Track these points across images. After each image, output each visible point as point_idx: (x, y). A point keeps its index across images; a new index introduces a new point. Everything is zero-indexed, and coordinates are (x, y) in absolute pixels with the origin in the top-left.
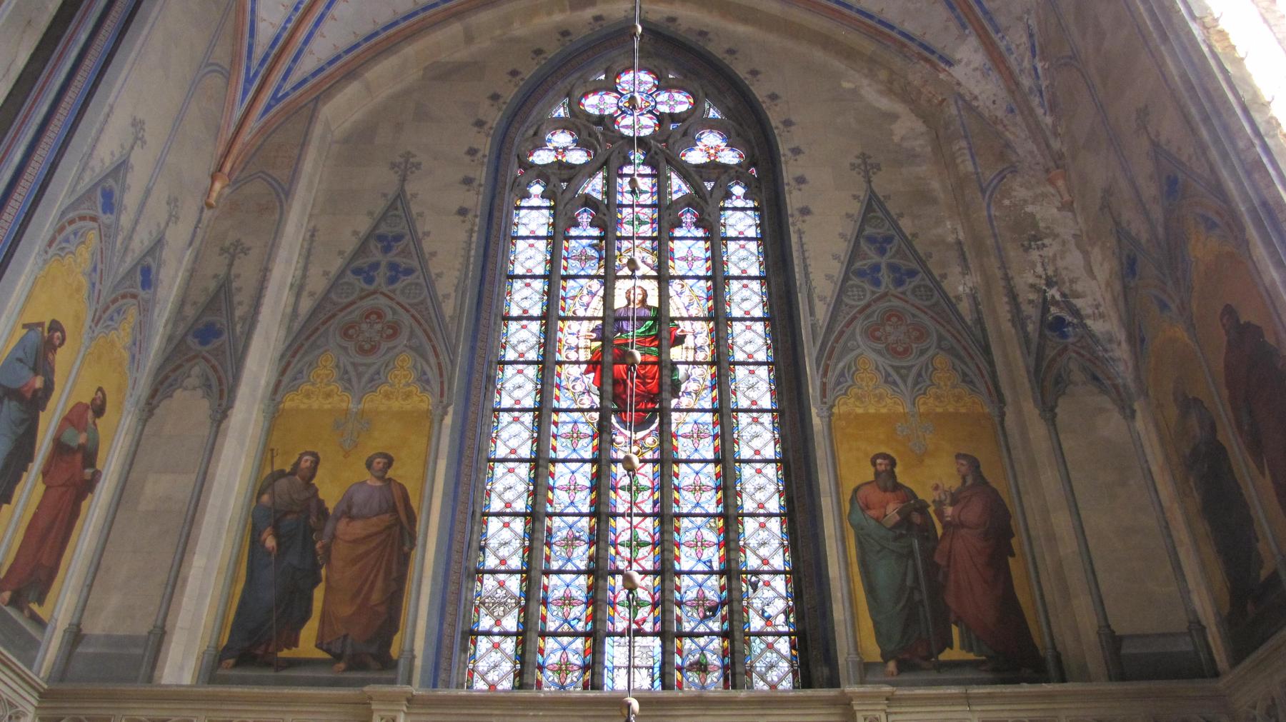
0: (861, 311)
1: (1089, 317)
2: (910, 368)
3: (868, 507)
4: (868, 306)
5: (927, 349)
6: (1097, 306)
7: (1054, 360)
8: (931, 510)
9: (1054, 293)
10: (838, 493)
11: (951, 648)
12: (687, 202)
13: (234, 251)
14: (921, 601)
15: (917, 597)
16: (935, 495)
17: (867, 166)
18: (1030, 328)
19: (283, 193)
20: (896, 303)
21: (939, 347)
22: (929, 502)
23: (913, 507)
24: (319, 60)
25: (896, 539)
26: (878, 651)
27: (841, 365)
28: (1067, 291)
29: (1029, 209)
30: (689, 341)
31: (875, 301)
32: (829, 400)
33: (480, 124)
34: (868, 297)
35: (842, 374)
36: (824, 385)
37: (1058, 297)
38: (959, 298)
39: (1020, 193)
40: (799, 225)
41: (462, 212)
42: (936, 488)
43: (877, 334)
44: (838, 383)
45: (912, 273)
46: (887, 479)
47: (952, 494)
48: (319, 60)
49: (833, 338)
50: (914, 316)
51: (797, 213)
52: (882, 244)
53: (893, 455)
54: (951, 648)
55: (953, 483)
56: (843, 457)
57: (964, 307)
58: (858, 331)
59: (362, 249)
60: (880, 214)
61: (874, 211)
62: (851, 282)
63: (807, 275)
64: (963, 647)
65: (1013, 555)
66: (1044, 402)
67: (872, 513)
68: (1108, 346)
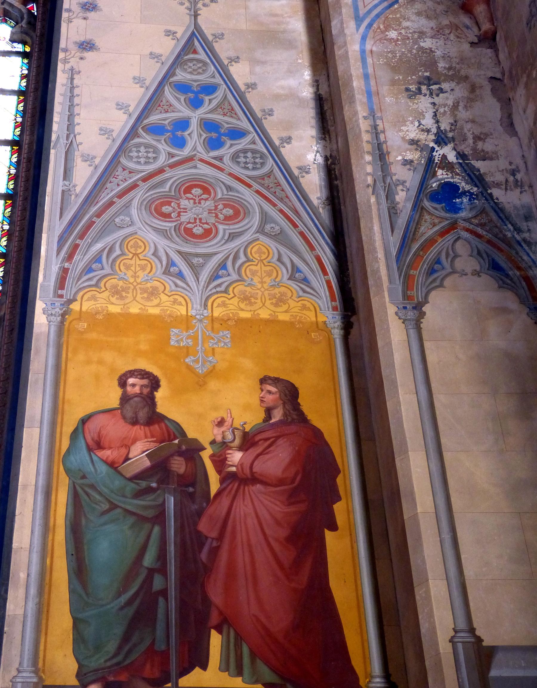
0: (145, 179)
1: (498, 185)
2: (208, 256)
3: (99, 445)
4: (161, 171)
5: (240, 234)
6: (513, 173)
7: (430, 242)
8: (206, 455)
10: (53, 424)
11: (204, 667)
14: (164, 593)
15: (158, 583)
16: (217, 434)
18: (401, 196)
20: (204, 170)
21: (261, 230)
22: (205, 440)
25: (139, 494)
26: (74, 666)
27: (98, 246)
28: (468, 151)
31: (172, 166)
32: (67, 293)
34: (162, 160)
35: (97, 259)
36: (65, 271)
37: (452, 157)
38: (305, 170)
40: (73, 62)
42: (221, 423)
43: (166, 209)
44: (88, 270)
45: (237, 134)
46: (141, 404)
47: (245, 435)
49: (93, 210)
50: (229, 188)
51: (72, 47)
52: (196, 96)
53: (156, 372)
54: (204, 667)
55: (250, 417)
56: (72, 373)
58: (135, 203)
60: (202, 56)
61: (195, 52)
62: (137, 140)
63: (71, 126)
64: (225, 667)
65: (334, 527)
66: (406, 297)
67: (107, 454)
68: (524, 225)
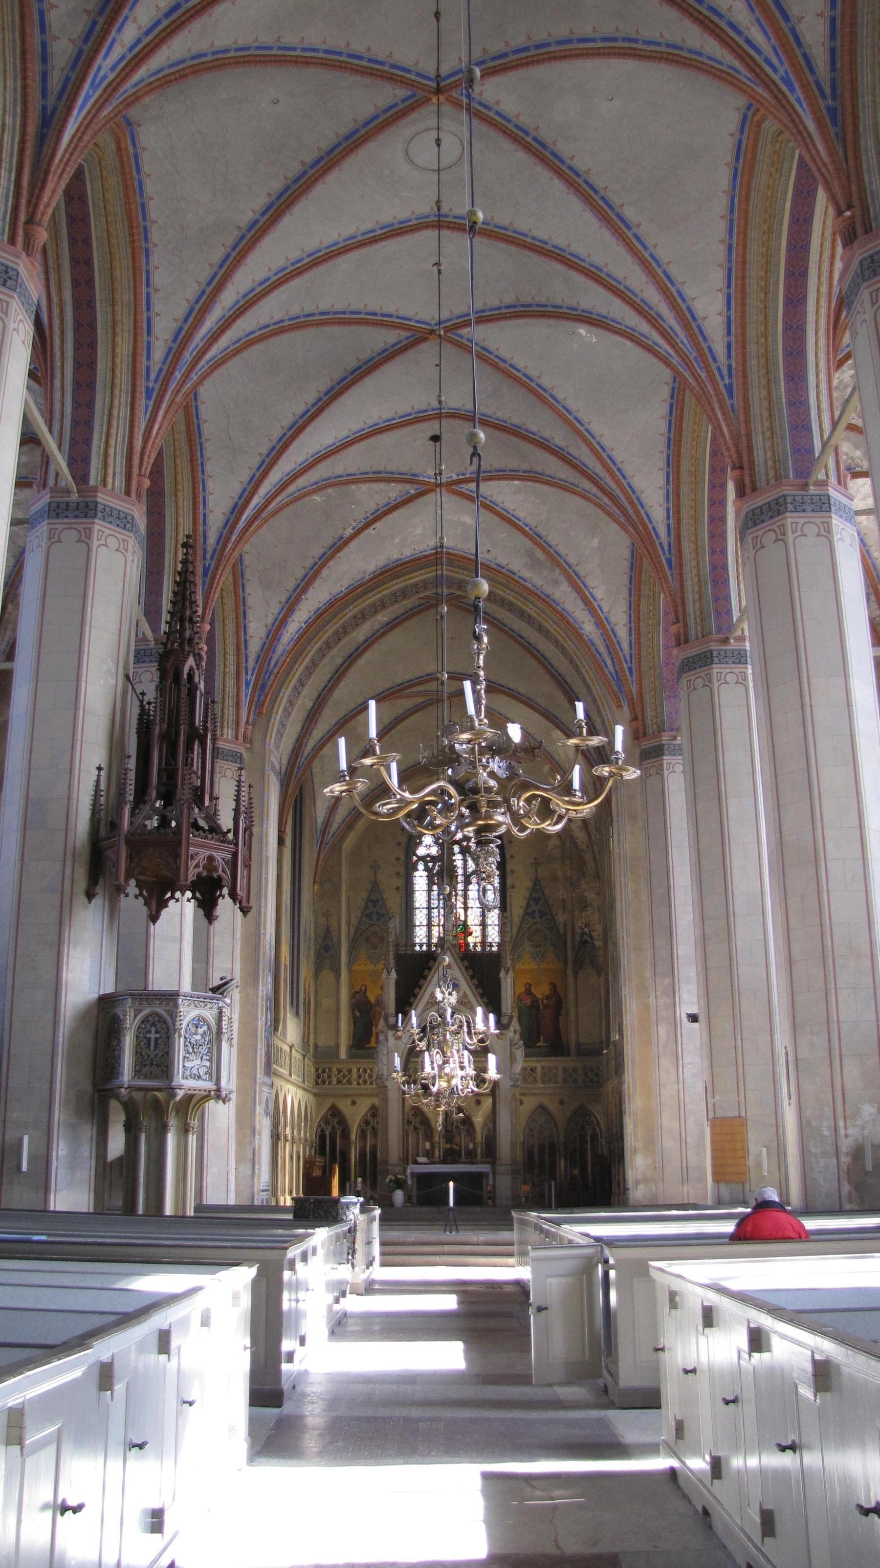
9: (586, 930)
12: (473, 873)
13: (327, 915)
17: (536, 864)
19: (338, 889)
23: (535, 1000)
24: (166, 341)
29: (586, 894)
30: (474, 934)
33: (399, 844)
39: (584, 886)
41: (398, 888)
46: (528, 992)
48: (166, 341)
52: (537, 901)
55: (547, 992)
57: (561, 927)
59: (366, 907)
